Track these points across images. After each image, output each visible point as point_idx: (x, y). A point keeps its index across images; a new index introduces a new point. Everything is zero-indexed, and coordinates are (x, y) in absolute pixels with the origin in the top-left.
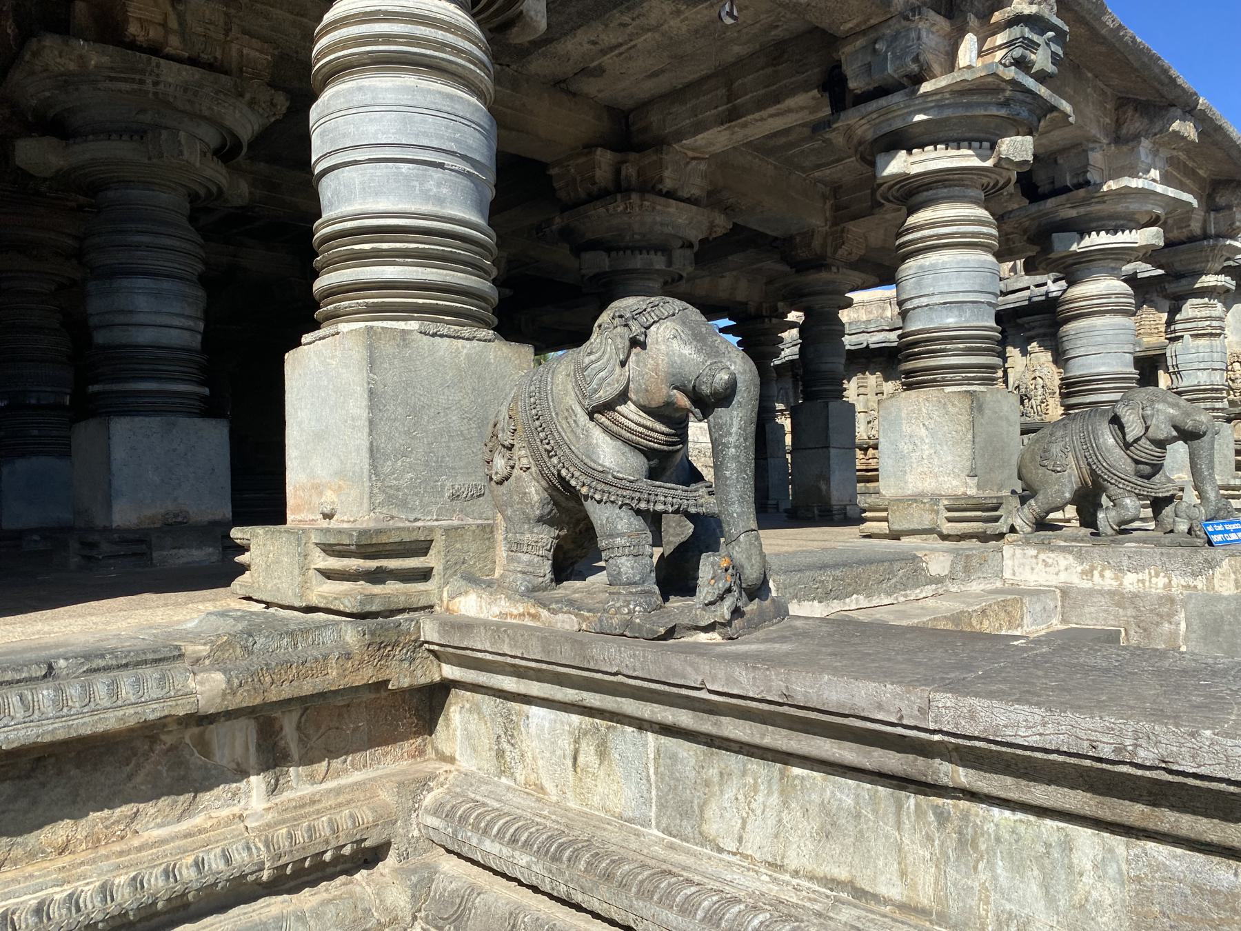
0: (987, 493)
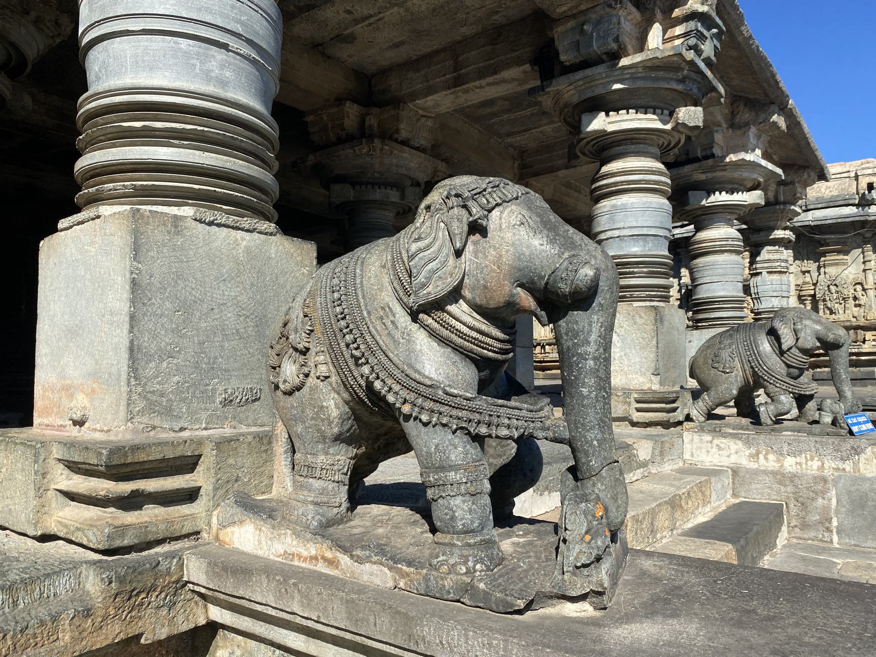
0: (667, 388)
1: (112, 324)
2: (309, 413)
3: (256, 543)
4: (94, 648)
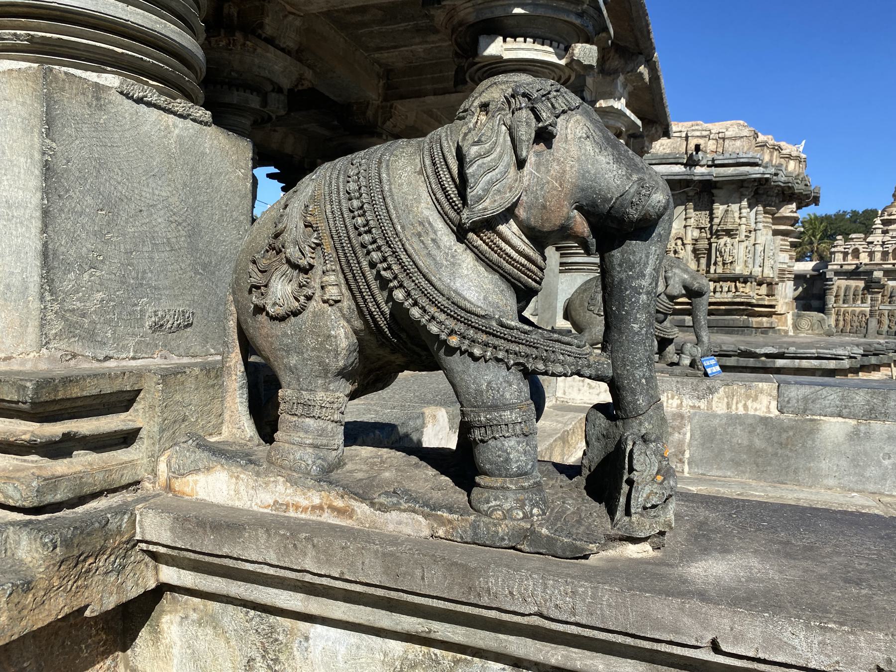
1: (9, 220)
2: (310, 341)
3: (232, 493)
4: (35, 628)
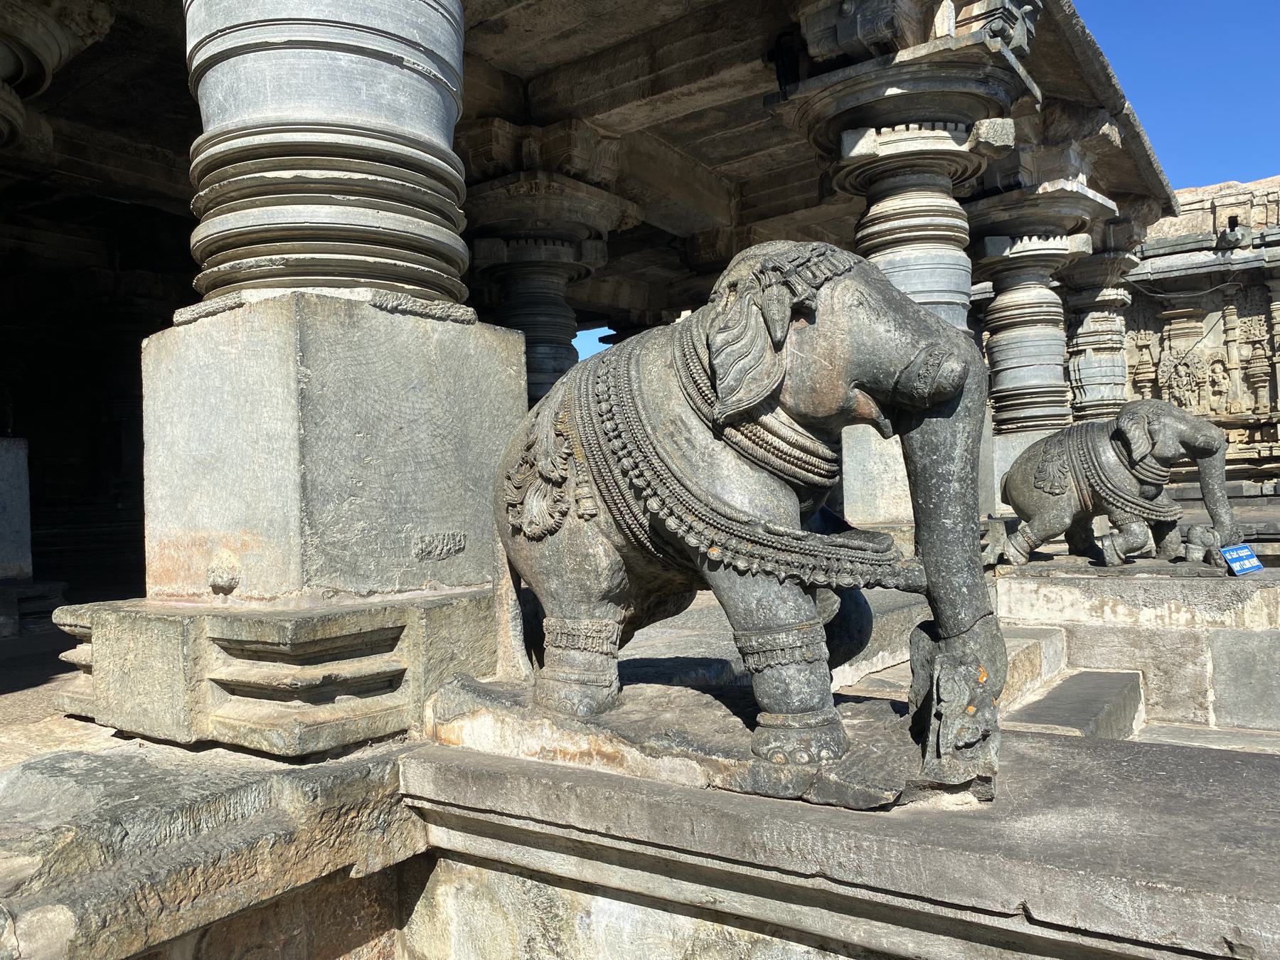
1: (270, 453)
2: (569, 562)
3: (498, 739)
4: (299, 884)
